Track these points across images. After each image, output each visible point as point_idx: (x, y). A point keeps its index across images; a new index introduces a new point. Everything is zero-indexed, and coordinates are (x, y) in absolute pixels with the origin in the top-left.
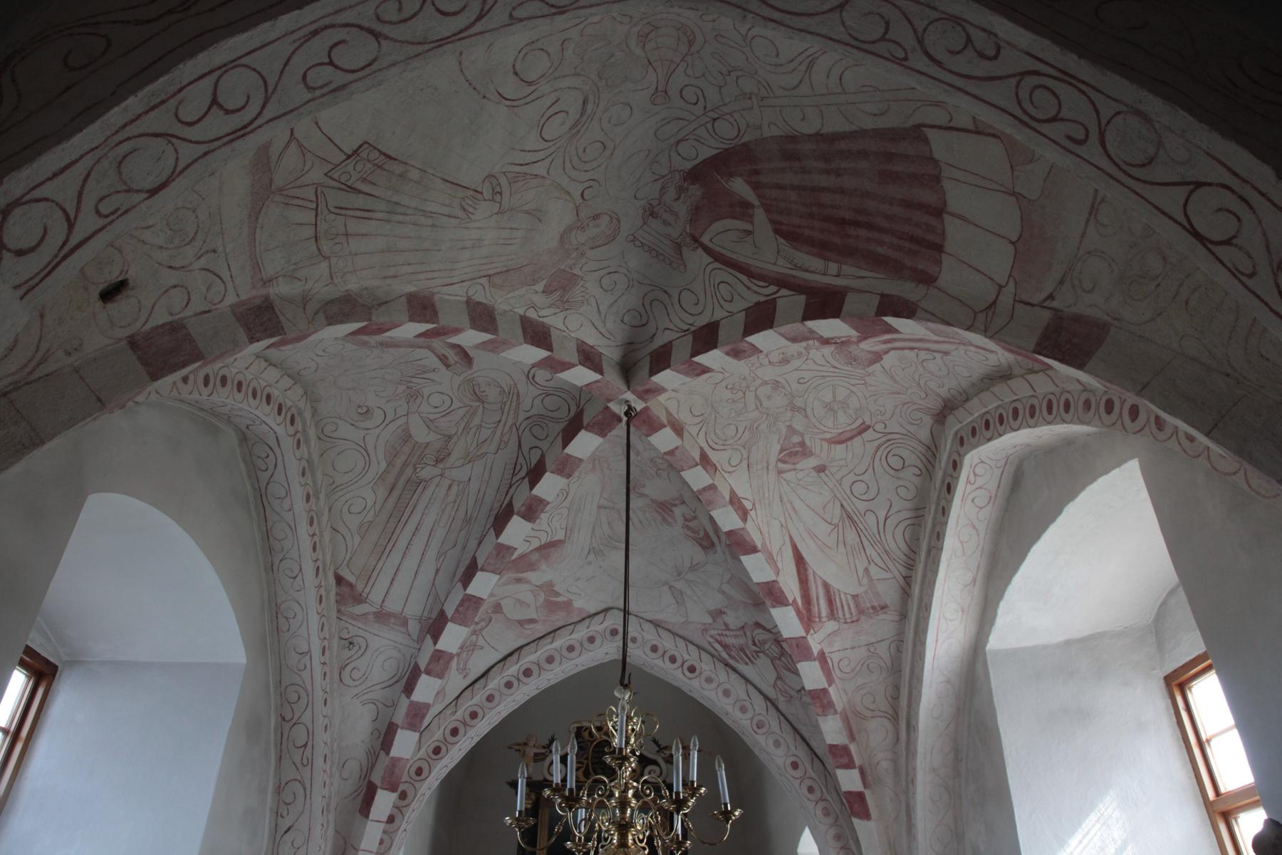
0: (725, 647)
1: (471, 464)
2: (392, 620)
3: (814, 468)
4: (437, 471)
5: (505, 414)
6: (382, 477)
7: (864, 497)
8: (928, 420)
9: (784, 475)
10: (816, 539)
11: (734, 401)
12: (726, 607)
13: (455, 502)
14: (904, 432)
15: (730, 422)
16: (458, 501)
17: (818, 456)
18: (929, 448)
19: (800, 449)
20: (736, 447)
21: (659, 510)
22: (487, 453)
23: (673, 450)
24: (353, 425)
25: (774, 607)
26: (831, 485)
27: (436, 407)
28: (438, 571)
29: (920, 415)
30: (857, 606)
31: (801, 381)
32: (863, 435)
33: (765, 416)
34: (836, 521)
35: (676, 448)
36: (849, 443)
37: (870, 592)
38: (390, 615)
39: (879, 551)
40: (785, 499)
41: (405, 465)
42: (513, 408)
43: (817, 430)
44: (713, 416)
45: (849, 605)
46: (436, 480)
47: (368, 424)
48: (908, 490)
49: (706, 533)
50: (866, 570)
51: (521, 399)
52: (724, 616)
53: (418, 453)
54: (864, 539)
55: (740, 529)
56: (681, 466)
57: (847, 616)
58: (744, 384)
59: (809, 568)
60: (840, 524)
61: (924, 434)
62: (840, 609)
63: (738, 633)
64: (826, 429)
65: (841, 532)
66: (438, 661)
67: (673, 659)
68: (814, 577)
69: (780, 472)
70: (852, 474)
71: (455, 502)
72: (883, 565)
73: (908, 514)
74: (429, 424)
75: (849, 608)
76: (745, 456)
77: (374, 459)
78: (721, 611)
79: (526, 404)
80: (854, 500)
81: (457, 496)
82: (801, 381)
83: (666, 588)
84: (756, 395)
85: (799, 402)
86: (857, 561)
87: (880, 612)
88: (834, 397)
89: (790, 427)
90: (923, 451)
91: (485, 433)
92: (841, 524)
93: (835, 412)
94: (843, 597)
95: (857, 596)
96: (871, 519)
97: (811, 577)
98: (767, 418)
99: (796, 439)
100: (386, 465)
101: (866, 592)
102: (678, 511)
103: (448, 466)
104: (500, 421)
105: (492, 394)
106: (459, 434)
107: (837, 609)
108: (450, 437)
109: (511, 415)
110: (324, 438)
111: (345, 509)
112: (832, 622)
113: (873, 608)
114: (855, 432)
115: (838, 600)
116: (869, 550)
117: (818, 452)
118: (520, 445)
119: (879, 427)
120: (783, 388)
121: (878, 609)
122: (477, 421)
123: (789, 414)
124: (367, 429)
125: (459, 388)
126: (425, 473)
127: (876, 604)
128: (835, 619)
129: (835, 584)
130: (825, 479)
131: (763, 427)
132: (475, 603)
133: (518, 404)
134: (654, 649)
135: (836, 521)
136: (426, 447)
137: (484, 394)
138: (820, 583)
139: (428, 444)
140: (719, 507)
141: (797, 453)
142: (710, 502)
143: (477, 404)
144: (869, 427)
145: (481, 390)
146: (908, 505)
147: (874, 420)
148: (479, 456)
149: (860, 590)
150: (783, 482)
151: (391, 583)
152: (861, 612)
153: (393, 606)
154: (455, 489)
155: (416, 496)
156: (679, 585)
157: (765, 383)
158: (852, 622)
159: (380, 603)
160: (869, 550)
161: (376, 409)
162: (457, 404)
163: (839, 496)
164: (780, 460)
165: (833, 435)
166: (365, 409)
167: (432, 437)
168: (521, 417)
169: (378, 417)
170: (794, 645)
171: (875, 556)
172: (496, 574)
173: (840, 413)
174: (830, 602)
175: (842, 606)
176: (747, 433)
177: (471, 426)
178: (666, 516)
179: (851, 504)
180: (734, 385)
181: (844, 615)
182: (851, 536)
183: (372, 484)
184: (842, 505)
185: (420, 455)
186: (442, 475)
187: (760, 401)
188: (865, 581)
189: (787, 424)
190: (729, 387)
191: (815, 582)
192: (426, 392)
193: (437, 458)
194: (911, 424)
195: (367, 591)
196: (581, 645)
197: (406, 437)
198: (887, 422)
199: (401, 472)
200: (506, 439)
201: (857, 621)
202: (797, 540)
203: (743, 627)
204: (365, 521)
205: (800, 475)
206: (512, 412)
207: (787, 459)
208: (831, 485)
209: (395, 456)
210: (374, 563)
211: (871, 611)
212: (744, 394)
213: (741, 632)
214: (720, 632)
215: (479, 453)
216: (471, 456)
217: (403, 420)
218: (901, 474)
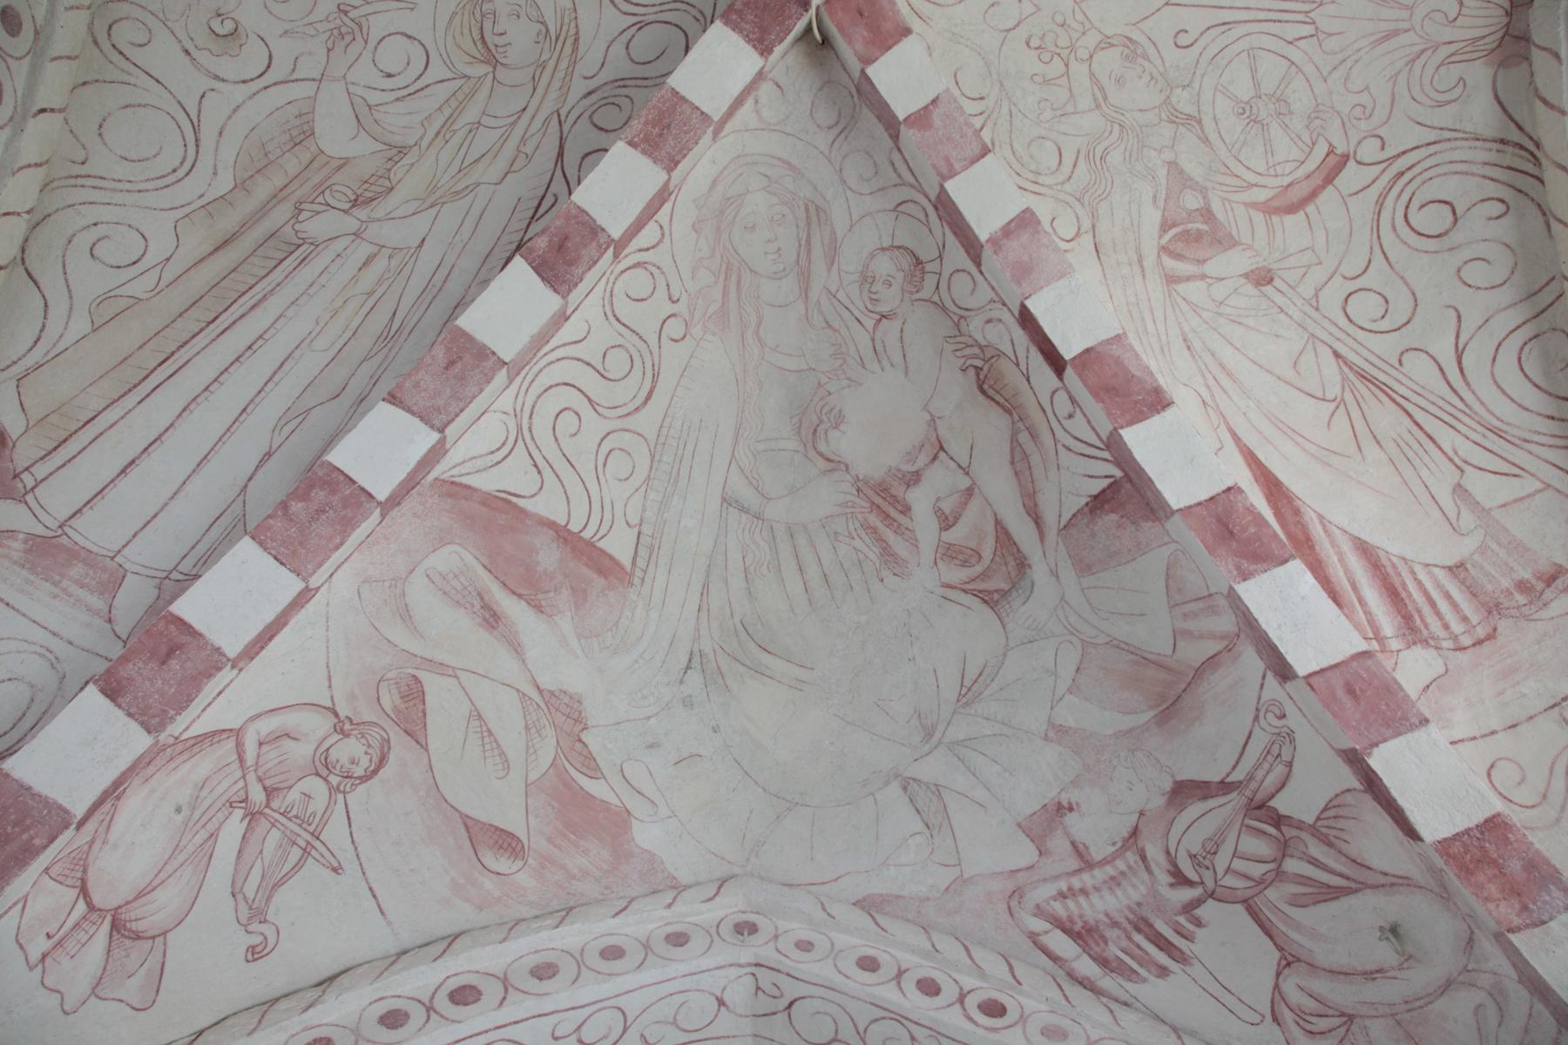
0: (1083, 935)
1: (433, 211)
2: (77, 570)
3: (1246, 276)
4: (351, 224)
5: (540, 91)
6: (210, 208)
7: (1384, 325)
8: (1479, 74)
9: (1181, 288)
10: (1300, 440)
11: (1047, 82)
12: (1075, 783)
13: (370, 294)
14: (1432, 136)
15: (1043, 133)
16: (377, 295)
17: (1250, 247)
18: (1502, 141)
19: (1204, 227)
20: (1062, 196)
21: (874, 520)
22: (478, 184)
23: (926, 108)
24: (187, 53)
25: (1245, 577)
26: (1297, 315)
27: (390, 76)
28: (269, 455)
29: (1455, 71)
30: (1473, 593)
31: (1184, 40)
32: (1337, 182)
33: (1116, 127)
34: (1334, 391)
35: (934, 101)
36: (1310, 209)
37: (1494, 546)
38: (77, 554)
39: (1474, 436)
40: (1197, 344)
41: (276, 197)
42: (560, 75)
43: (1229, 180)
44: (1005, 110)
45: (1448, 596)
46: (339, 245)
47: (226, 67)
48: (1488, 262)
49: (1003, 536)
50: (1459, 490)
51: (581, 52)
52: (1070, 819)
53: (316, 179)
54: (1419, 416)
55: (1108, 341)
56: (947, 159)
57: (1457, 627)
58: (1063, 42)
59: (1303, 509)
60: (1348, 397)
61: (1480, 114)
62: (1427, 610)
63: (1120, 865)
64: (1251, 178)
65: (1356, 414)
66: (163, 663)
67: (929, 988)
68: (1326, 531)
69: (1171, 280)
70: (1337, 280)
71: (370, 294)
72: (1506, 468)
73: (1513, 317)
74: (363, 116)
75: (1455, 606)
76: (1086, 224)
77: (206, 161)
78: (1060, 806)
79: (590, 59)
80: (1360, 335)
81: (379, 282)
82: (1184, 40)
83: (895, 788)
84: (1092, 74)
85: (1183, 100)
86: (1424, 473)
87: (1548, 594)
88: (1257, 85)
89: (1172, 165)
90: (1493, 157)
91: (486, 139)
92: (1348, 397)
93: (1264, 127)
94: (1422, 576)
95: (1461, 565)
96: (1419, 368)
97: (1317, 531)
98: (1120, 138)
99: (1192, 201)
100: (231, 186)
101: (1483, 549)
102: (921, 500)
103: (379, 213)
104: (524, 109)
105: (519, 39)
106: (424, 144)
107: (1419, 611)
108: (402, 151)
109: (553, 95)
110: (106, 46)
111: (86, 239)
112: (1418, 650)
113: (1523, 586)
114: (1317, 180)
115: (1412, 587)
116: (1446, 438)
117: (1245, 237)
118: (561, 154)
119: (1369, 151)
120: (1146, 57)
121: (1540, 586)
122: (472, 114)
123: (1167, 130)
124: (216, 77)
125: (450, 22)
126: (316, 227)
127: (1526, 575)
128: (1425, 642)
129: (1391, 545)
130: (1279, 299)
131: (1115, 157)
132: (346, 503)
133: (574, 63)
134: (869, 964)
135: (1334, 391)
136: (339, 168)
137: (500, 41)
138: (1347, 547)
139: (345, 162)
140: (1048, 283)
141: (1199, 236)
142: (1023, 271)
143: (486, 69)
144: (1345, 158)
145: (498, 29)
146: (1505, 296)
147: (1354, 137)
148: (458, 193)
149: (1462, 548)
150: (1183, 305)
151: (123, 471)
152: (1493, 609)
153: (96, 532)
154: (379, 266)
155: (277, 275)
156: (934, 768)
157: (1107, 43)
158: (1479, 643)
159: (63, 514)
160: (1446, 438)
161: (253, 38)
162: (437, 70)
163: (1323, 336)
164: (1164, 249)
165: (1271, 193)
166: (229, 26)
167: (363, 146)
168: (574, 95)
169: (251, 59)
170: (1340, 693)
171: (1466, 450)
172: (432, 427)
173: (1275, 130)
174: (1394, 595)
175: (1433, 604)
176: (1082, 164)
177: (455, 127)
178: (890, 536)
179: (1356, 346)
180: (1042, 38)
181: (1446, 627)
182: (1386, 418)
183: (179, 213)
184: (1337, 355)
185: (321, 183)
186: (357, 235)
187: (1102, 89)
188: (1467, 520)
189: (1168, 155)
190: (1035, 42)
191: (1333, 543)
192: (377, 27)
193: (356, 200)
194: (1441, 104)
195: (41, 470)
196: (646, 946)
197: (301, 133)
198: (1382, 132)
199: (263, 211)
200: (529, 149)
201: (1491, 636)
202: (1251, 441)
203: (1135, 833)
204: (127, 290)
205: (1220, 290)
206: (556, 84)
207: (1179, 247)
208: (1297, 315)
209: (259, 171)
210: (95, 404)
211: (1521, 599)
212: (1067, 65)
213: (1131, 857)
214: (1063, 886)
215: (459, 187)
216: (439, 193)
217: (307, 89)
218: (1457, 237)
